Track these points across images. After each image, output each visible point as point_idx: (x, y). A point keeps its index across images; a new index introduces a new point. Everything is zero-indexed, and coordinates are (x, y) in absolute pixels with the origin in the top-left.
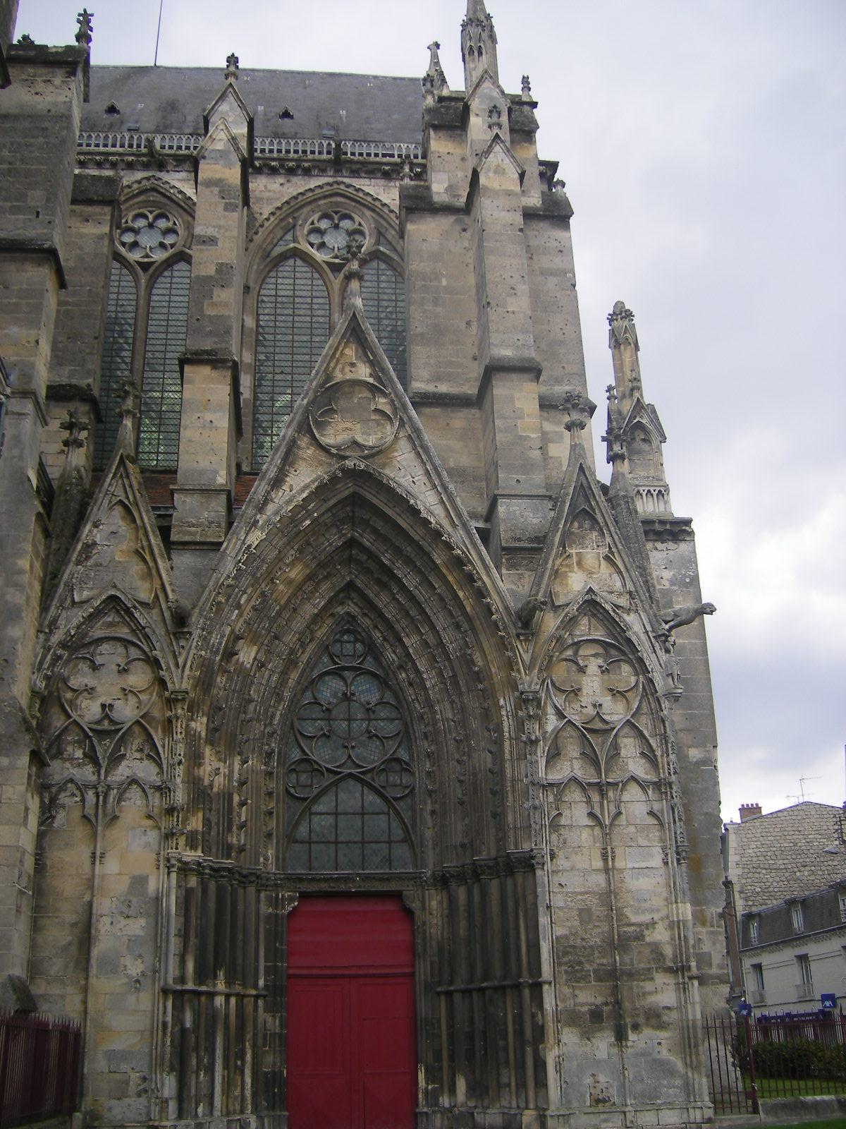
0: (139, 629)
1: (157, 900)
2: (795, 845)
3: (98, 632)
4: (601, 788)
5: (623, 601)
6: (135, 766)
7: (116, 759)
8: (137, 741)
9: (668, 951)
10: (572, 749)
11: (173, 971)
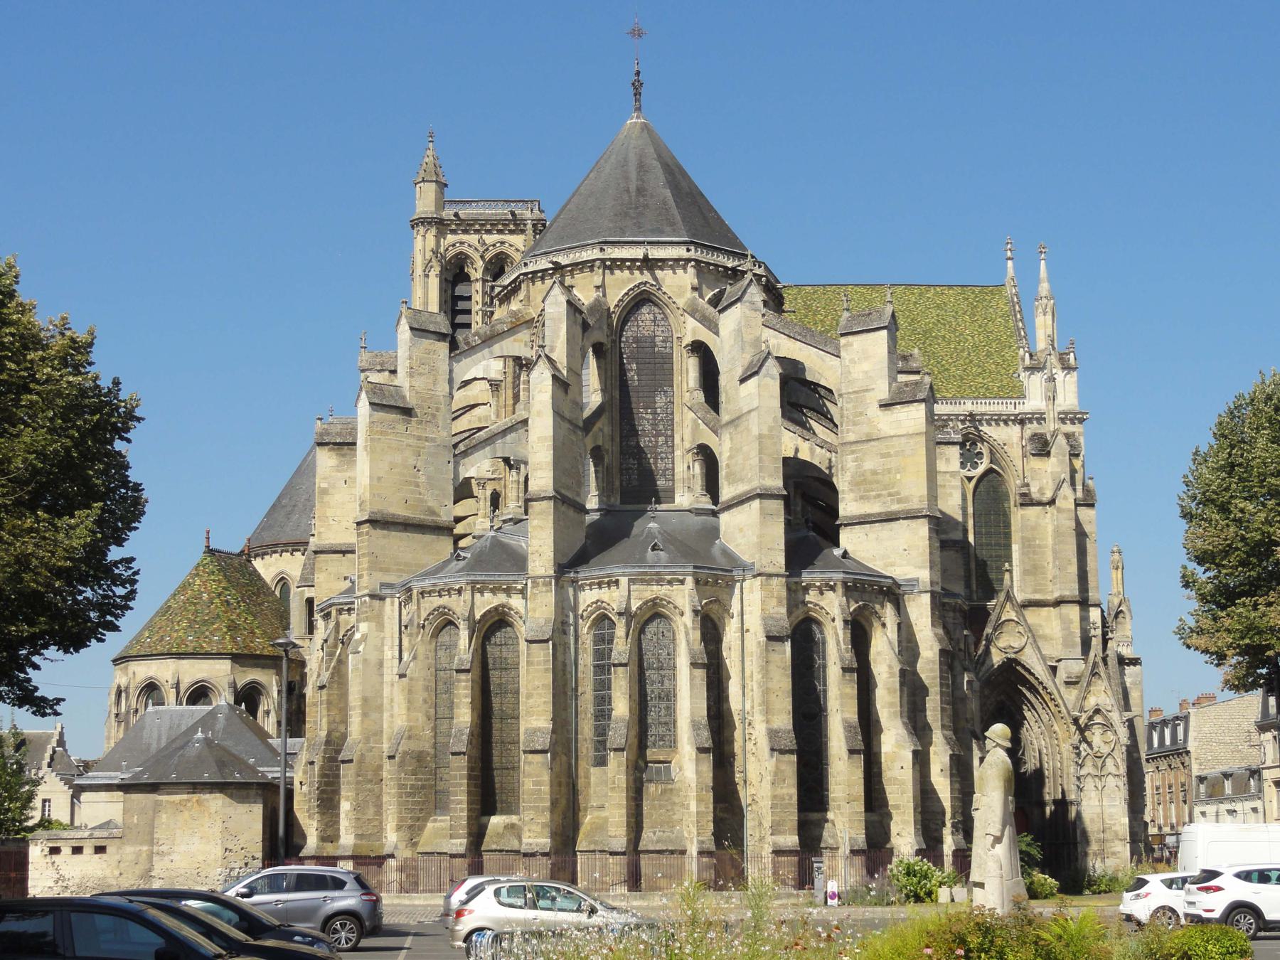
2: (1240, 725)
4: (1100, 777)
5: (1109, 708)
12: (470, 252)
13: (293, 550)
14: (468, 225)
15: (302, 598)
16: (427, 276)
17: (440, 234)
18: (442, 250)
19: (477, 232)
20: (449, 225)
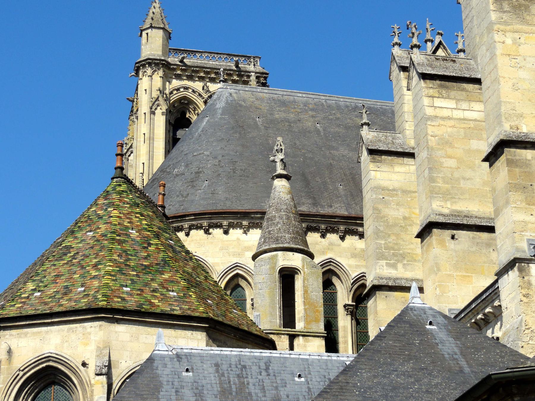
12: (194, 97)
13: (211, 226)
14: (193, 71)
15: (273, 268)
16: (153, 113)
17: (166, 78)
18: (167, 92)
19: (201, 79)
20: (174, 70)
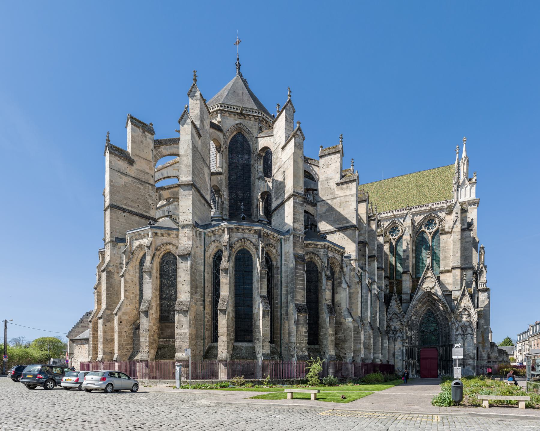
0: (398, 317)
1: (402, 350)
3: (393, 317)
6: (399, 334)
7: (396, 334)
8: (399, 332)
9: (472, 357)
10: (460, 330)
11: (405, 358)
